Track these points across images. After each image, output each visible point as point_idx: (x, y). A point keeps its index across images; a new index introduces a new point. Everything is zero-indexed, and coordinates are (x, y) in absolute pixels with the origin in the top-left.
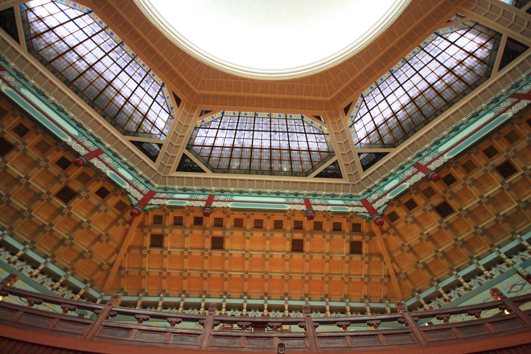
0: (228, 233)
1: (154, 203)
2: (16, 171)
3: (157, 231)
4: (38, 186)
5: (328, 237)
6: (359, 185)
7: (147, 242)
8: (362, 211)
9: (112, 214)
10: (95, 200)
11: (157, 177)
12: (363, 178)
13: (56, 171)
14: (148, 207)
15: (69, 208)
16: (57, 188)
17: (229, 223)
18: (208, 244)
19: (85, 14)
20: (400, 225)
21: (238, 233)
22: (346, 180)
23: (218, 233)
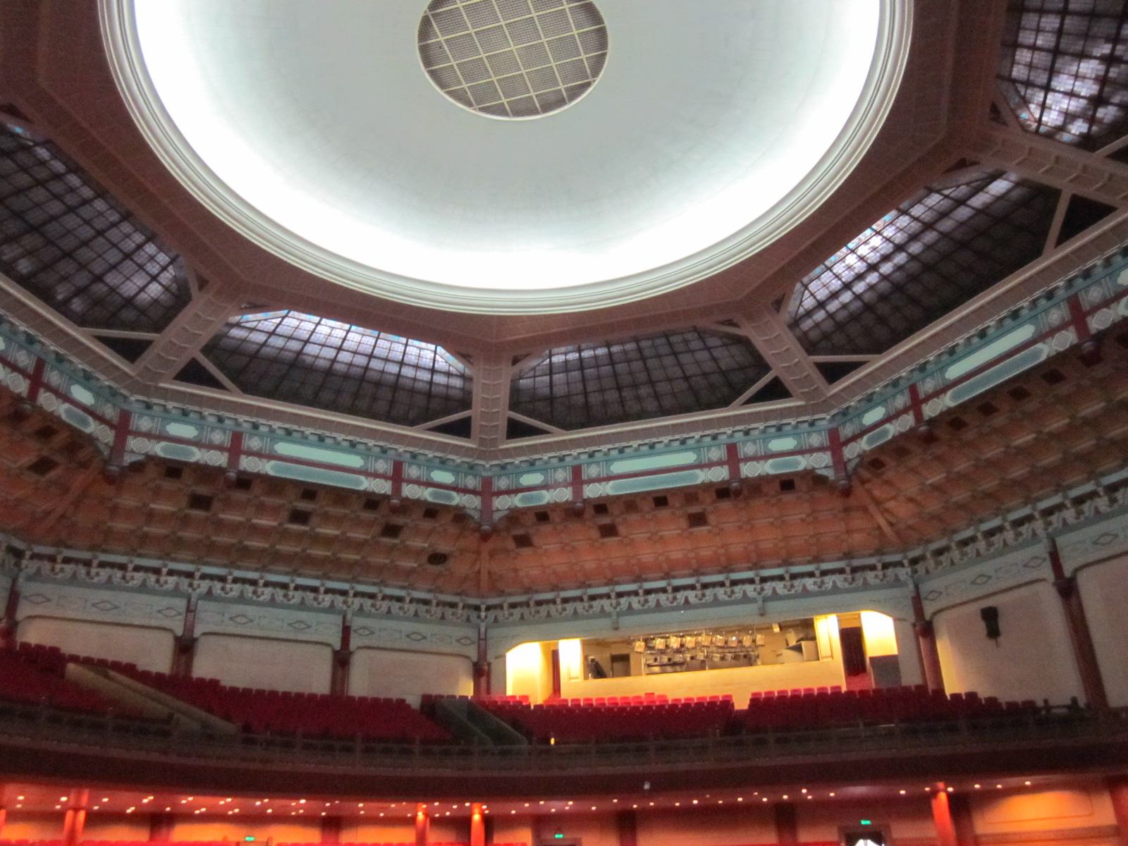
0: (618, 520)
1: (500, 508)
2: (329, 531)
3: (520, 532)
4: (358, 535)
5: (774, 501)
6: (825, 406)
7: (511, 544)
8: (823, 466)
9: (453, 530)
10: (427, 524)
11: (483, 455)
12: (829, 395)
13: (367, 515)
14: (496, 516)
15: (403, 542)
16: (376, 530)
17: (615, 510)
18: (595, 534)
19: (283, 318)
20: (890, 474)
21: (634, 517)
22: (801, 399)
23: (605, 520)
